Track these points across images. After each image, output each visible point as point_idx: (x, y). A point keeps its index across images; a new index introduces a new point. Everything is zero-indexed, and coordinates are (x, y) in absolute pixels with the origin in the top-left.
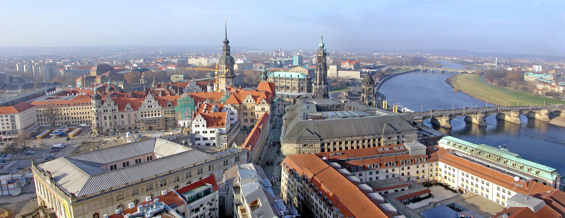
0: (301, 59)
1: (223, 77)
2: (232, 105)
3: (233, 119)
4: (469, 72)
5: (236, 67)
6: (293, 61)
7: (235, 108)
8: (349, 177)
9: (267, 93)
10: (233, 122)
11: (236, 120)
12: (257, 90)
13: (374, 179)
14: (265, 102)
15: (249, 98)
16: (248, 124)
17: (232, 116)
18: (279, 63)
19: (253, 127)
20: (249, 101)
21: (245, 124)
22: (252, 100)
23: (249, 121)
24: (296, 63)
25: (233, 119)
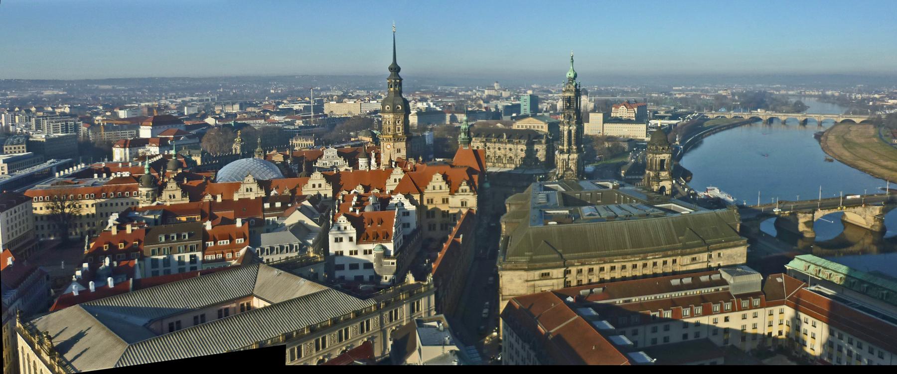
0: (535, 101)
1: (388, 140)
2: (406, 197)
3: (408, 225)
4: (858, 120)
5: (413, 120)
6: (519, 105)
7: (413, 202)
8: (611, 338)
9: (470, 171)
10: (408, 231)
11: (413, 226)
12: (452, 166)
13: (660, 342)
14: (468, 188)
15: (437, 180)
16: (437, 234)
17: (406, 220)
18: (493, 110)
19: (445, 239)
20: (437, 188)
21: (431, 234)
22: (444, 184)
23: (438, 227)
24: (526, 108)
25: (408, 225)
